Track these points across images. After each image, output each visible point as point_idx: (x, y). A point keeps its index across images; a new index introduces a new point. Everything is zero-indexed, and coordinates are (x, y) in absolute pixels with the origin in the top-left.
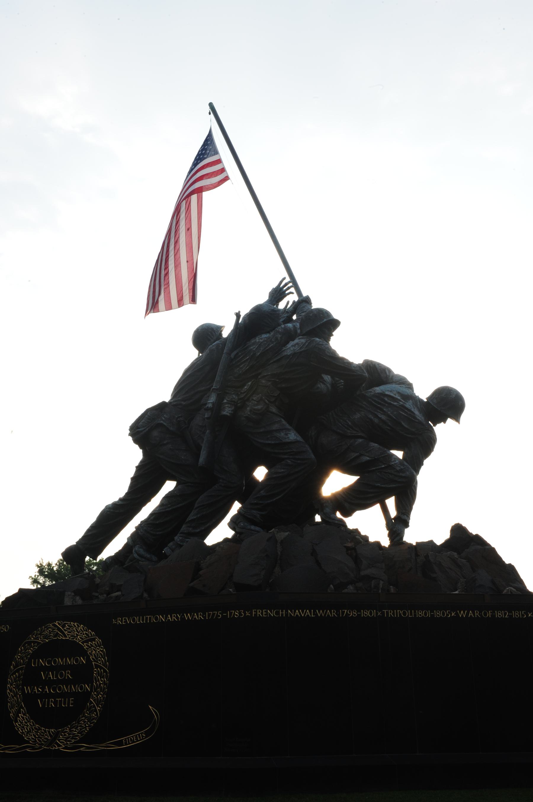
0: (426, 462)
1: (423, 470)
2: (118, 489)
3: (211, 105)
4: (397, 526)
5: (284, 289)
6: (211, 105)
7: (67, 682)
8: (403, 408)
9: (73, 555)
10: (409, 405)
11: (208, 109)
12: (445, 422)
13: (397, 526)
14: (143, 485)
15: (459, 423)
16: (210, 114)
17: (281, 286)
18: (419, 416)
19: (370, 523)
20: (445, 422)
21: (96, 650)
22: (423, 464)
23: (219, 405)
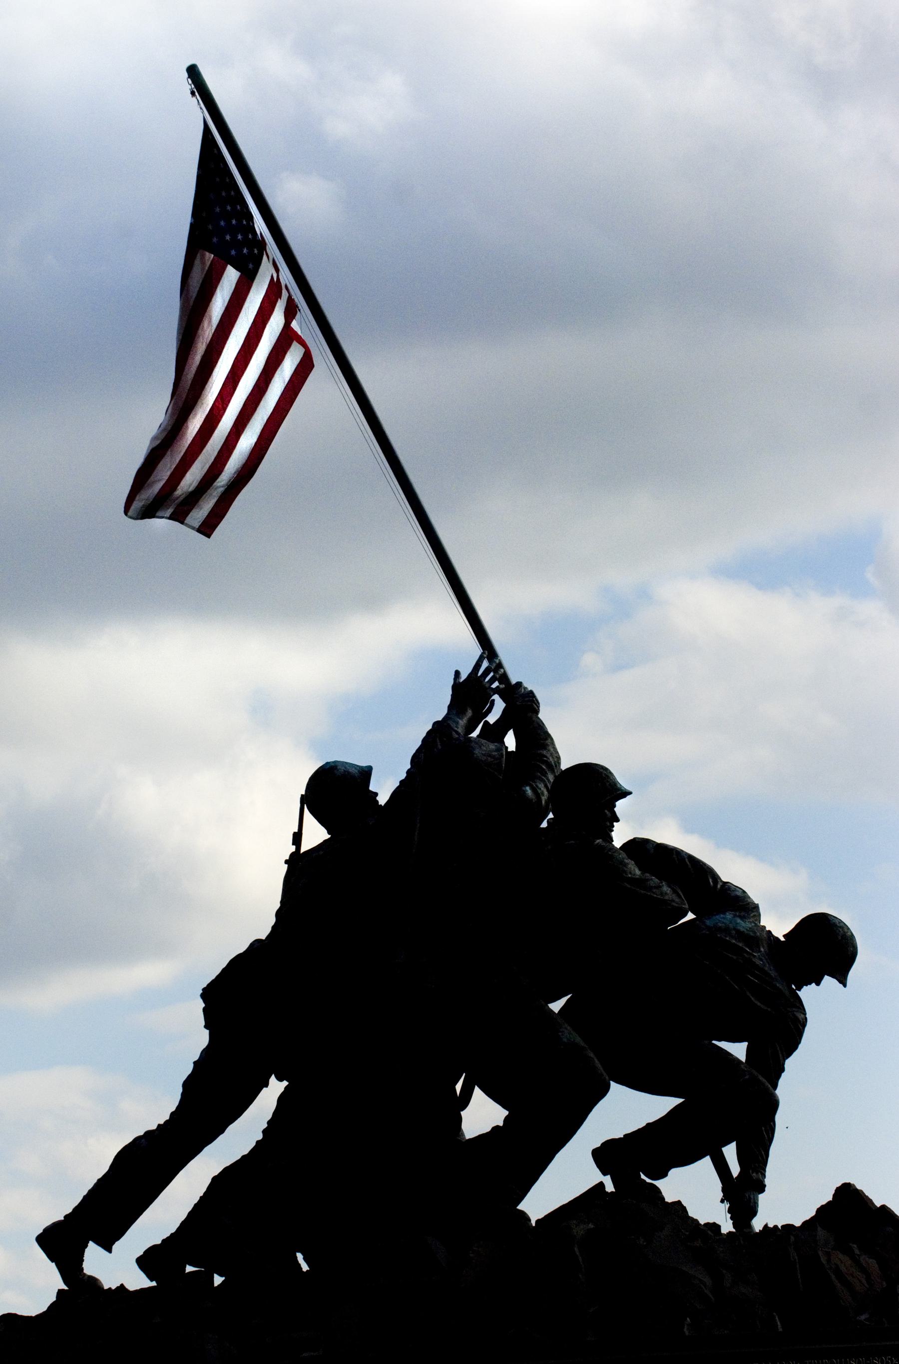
0: (790, 1063)
1: (782, 1082)
2: (155, 1106)
3: (193, 72)
4: (742, 1193)
5: (487, 679)
6: (193, 72)
9: (62, 1243)
10: (759, 957)
11: (186, 85)
12: (818, 984)
13: (742, 1193)
15: (845, 986)
16: (193, 93)
17: (480, 674)
19: (695, 1189)
20: (818, 984)
22: (783, 1070)
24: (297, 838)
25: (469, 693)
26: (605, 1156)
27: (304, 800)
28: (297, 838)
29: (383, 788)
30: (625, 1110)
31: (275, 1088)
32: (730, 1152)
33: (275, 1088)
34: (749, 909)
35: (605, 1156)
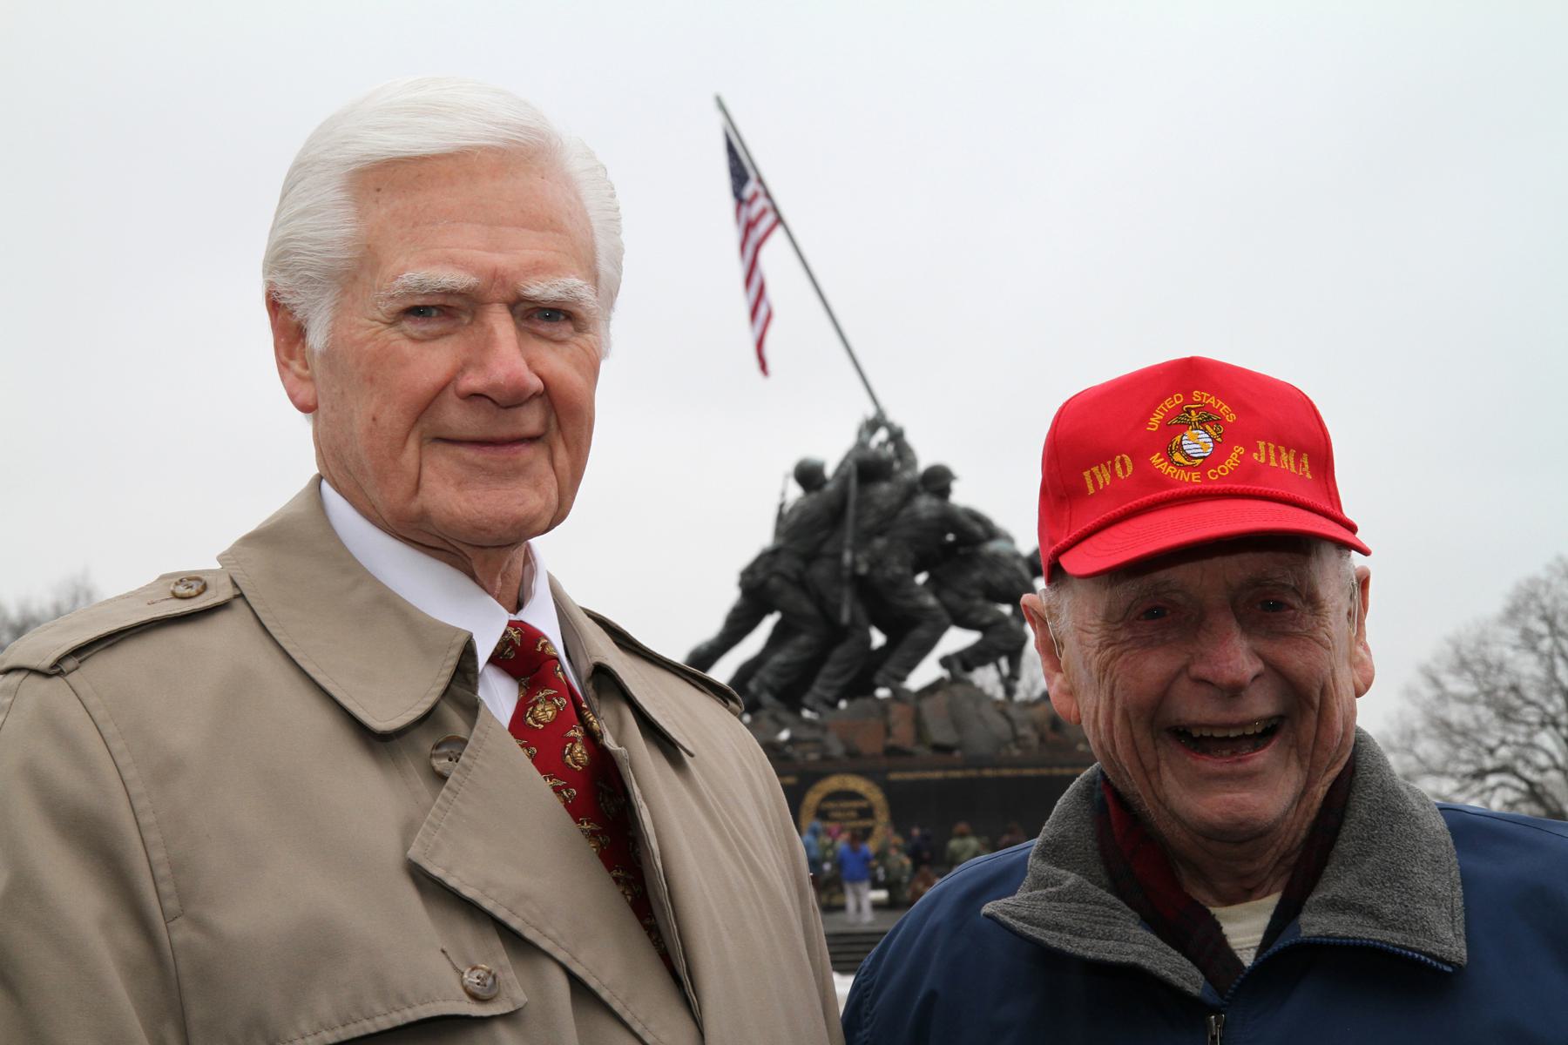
4: (1009, 682)
7: (852, 819)
8: (1015, 569)
10: (1020, 564)
11: (713, 105)
13: (1009, 682)
14: (738, 626)
18: (1026, 573)
19: (987, 678)
21: (875, 796)
23: (854, 564)
24: (783, 494)
25: (873, 425)
26: (945, 662)
27: (787, 476)
28: (783, 494)
29: (829, 471)
30: (957, 639)
31: (769, 623)
32: (1004, 662)
33: (769, 623)
34: (1010, 539)
35: (945, 662)
